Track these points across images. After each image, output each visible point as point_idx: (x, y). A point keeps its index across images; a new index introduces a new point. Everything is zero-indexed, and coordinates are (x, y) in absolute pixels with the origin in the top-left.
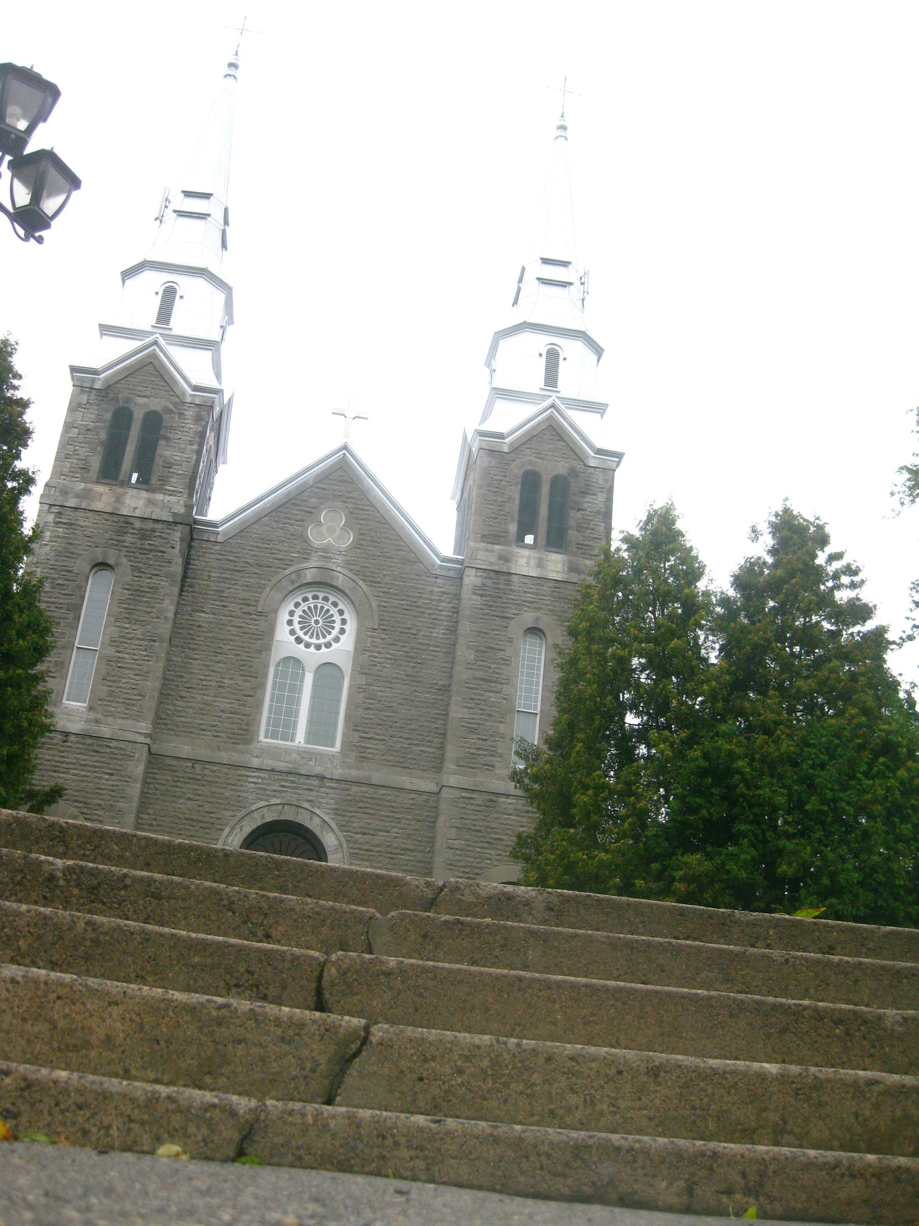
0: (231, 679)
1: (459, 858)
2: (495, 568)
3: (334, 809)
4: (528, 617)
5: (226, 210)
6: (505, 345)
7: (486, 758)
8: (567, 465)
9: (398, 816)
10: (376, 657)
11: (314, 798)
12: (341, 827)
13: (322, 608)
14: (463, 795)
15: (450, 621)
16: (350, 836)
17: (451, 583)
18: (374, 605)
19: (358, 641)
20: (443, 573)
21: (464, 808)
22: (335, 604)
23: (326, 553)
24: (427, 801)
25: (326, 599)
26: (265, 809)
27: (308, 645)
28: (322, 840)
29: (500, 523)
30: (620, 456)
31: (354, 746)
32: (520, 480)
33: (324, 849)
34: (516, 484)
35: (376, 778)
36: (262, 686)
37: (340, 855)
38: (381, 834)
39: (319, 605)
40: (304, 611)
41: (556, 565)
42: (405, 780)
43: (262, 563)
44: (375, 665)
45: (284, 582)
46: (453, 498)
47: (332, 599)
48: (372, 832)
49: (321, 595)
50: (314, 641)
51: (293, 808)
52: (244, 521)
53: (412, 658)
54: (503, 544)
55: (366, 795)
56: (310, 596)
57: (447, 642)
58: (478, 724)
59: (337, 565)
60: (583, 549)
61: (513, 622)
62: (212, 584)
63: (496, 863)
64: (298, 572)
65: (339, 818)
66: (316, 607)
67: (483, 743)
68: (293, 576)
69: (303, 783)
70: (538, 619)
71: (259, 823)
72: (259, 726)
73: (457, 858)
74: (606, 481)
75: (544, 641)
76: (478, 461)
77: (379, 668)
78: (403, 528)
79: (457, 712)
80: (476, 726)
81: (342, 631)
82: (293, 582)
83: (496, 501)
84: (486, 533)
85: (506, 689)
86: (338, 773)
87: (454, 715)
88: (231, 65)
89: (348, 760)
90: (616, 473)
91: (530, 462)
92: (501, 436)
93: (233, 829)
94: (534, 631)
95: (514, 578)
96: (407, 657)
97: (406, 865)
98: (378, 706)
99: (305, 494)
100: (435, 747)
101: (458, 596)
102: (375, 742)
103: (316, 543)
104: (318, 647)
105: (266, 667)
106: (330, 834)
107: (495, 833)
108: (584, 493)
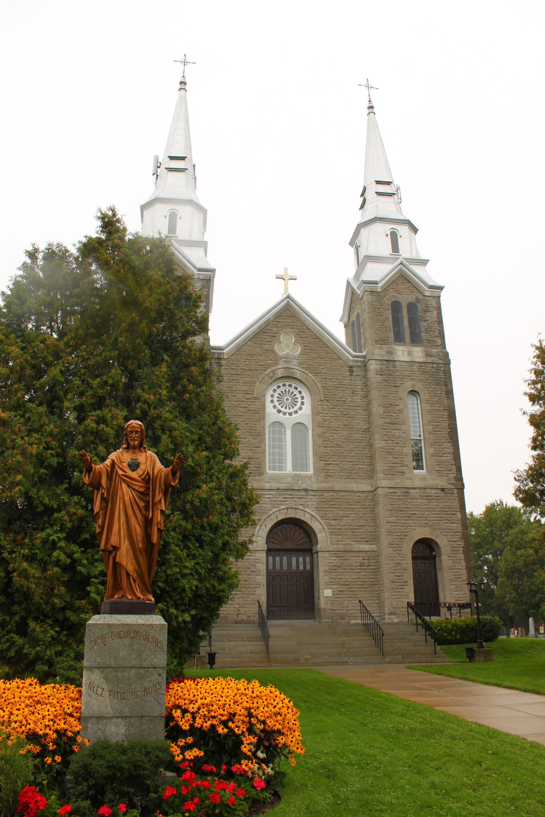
0: (245, 438)
1: (394, 528)
2: (386, 358)
3: (316, 508)
4: (409, 385)
5: (194, 166)
6: (364, 232)
7: (399, 468)
8: (414, 296)
9: (352, 507)
10: (325, 416)
11: (304, 503)
12: (321, 517)
13: (289, 391)
14: (390, 491)
15: (362, 391)
16: (329, 522)
17: (359, 369)
18: (319, 386)
19: (313, 408)
20: (354, 364)
21: (392, 498)
22: (296, 388)
23: (287, 359)
24: (367, 496)
25: (290, 386)
26: (277, 513)
27: (284, 414)
28: (313, 527)
29: (383, 332)
30: (441, 288)
31: (321, 469)
32: (390, 307)
33: (314, 532)
34: (389, 309)
35: (337, 487)
36: (263, 441)
37: (324, 534)
38: (345, 518)
39: (287, 390)
40: (279, 394)
41: (418, 353)
42: (354, 486)
43: (251, 368)
44: (325, 421)
45: (266, 378)
46: (340, 321)
47: (294, 385)
48: (340, 518)
49: (287, 384)
50: (287, 411)
51: (293, 510)
52: (238, 345)
53: (346, 414)
54: (388, 344)
55: (333, 497)
56: (281, 385)
57: (364, 403)
58: (392, 449)
59: (294, 364)
60: (431, 343)
61: (401, 388)
62: (225, 384)
63: (414, 528)
64: (273, 372)
65: (320, 512)
66: (285, 391)
67: (395, 459)
68: (271, 374)
69: (297, 495)
70: (414, 385)
71: (275, 521)
72: (266, 465)
73: (393, 528)
74: (436, 303)
75: (418, 398)
76: (365, 298)
77: (328, 423)
78: (328, 340)
79: (379, 443)
80: (391, 450)
81: (303, 403)
82: (271, 378)
83: (379, 320)
84: (377, 339)
85: (403, 427)
86: (315, 486)
87: (378, 445)
88: (181, 83)
89: (319, 478)
90: (442, 299)
91: (394, 296)
92: (376, 283)
93: (261, 526)
94: (413, 392)
95: (397, 363)
96: (342, 414)
97: (362, 535)
98: (331, 444)
99: (270, 326)
100: (367, 465)
101: (365, 376)
102: (333, 466)
103: (281, 354)
104: (290, 414)
105: (264, 429)
106: (317, 523)
107: (411, 511)
108: (426, 311)
